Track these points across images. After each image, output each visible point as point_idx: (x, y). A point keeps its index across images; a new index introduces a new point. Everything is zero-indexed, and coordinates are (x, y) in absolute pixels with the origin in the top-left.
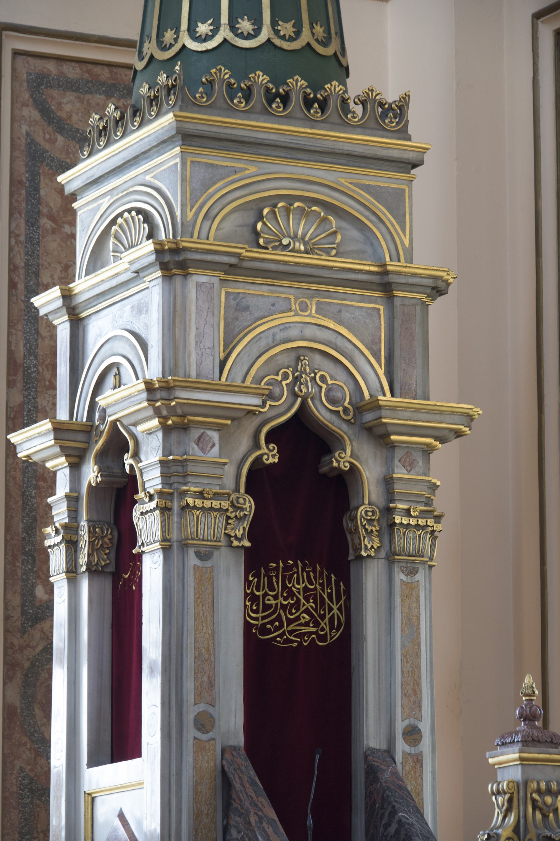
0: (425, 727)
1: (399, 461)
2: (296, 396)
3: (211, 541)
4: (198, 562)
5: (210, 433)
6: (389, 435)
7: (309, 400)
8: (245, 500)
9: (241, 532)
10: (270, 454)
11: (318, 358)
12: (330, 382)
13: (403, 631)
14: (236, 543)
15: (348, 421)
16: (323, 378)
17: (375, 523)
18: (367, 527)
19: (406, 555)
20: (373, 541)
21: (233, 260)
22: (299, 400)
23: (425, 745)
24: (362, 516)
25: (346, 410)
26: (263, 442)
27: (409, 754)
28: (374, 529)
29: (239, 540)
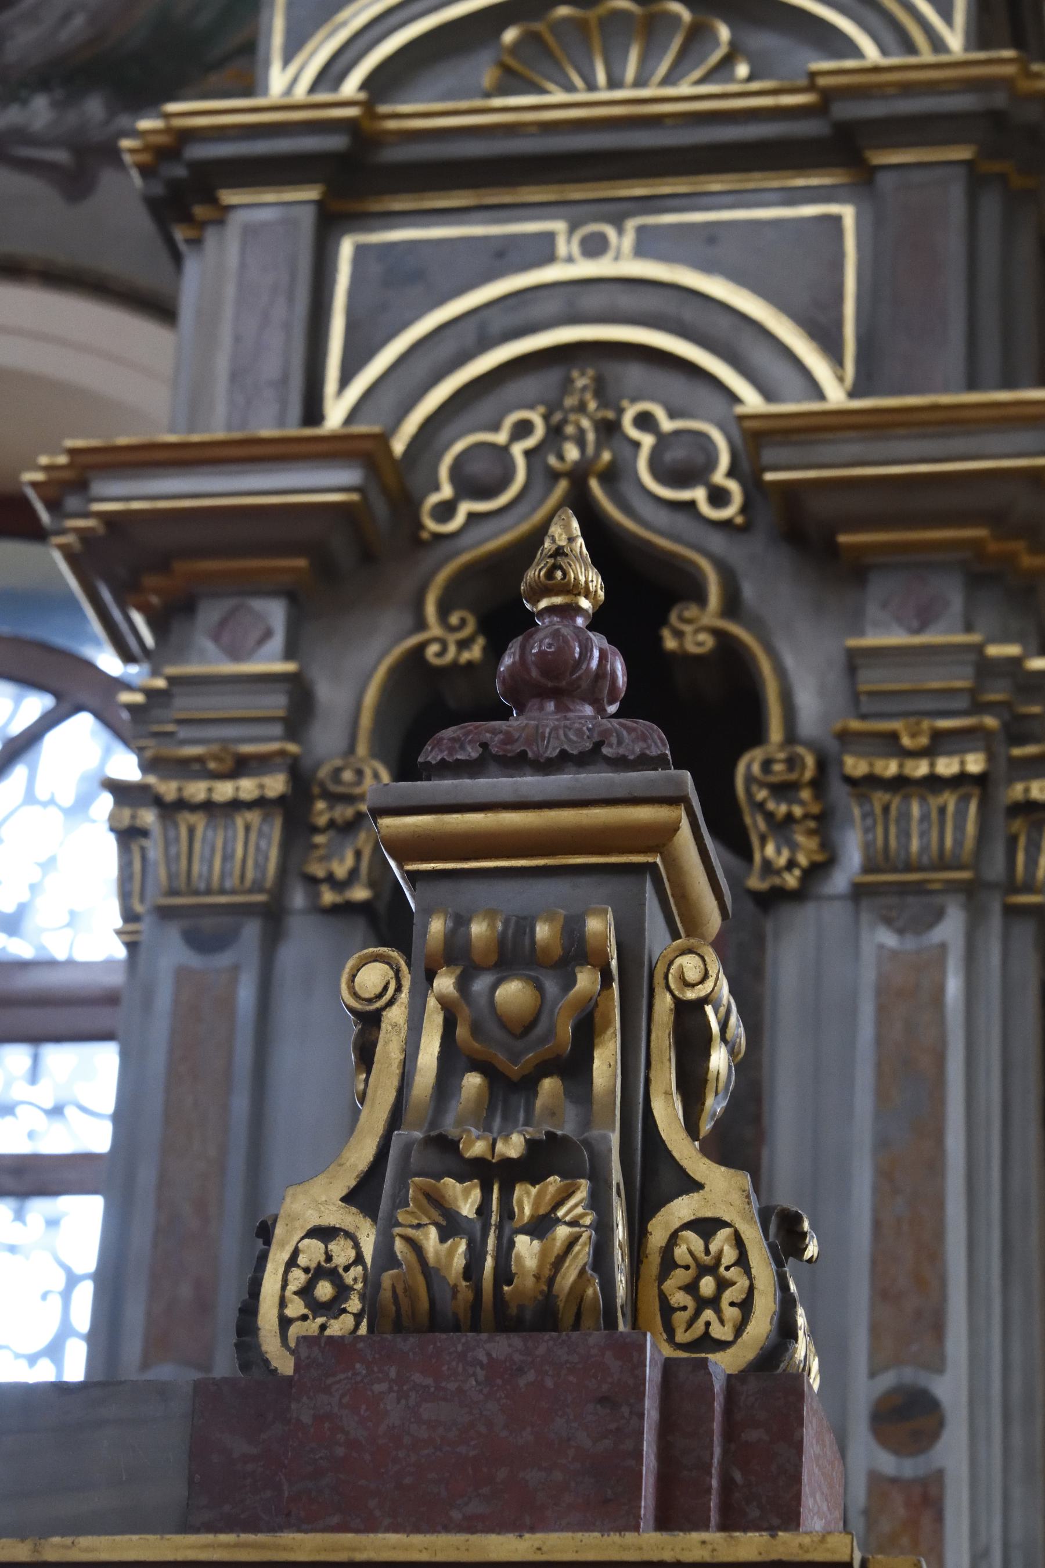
0: (950, 1389)
1: (884, 606)
2: (555, 476)
3: (233, 892)
4: (192, 960)
5: (259, 604)
6: (833, 535)
7: (594, 484)
8: (360, 773)
9: (349, 861)
10: (452, 639)
11: (635, 373)
12: (667, 425)
13: (881, 1095)
14: (328, 897)
15: (726, 525)
16: (645, 421)
17: (805, 794)
18: (771, 806)
19: (895, 870)
20: (794, 847)
21: (336, 143)
22: (563, 485)
23: (952, 1452)
24: (750, 779)
25: (719, 497)
26: (431, 609)
27: (894, 1481)
28: (798, 811)
29: (339, 885)
